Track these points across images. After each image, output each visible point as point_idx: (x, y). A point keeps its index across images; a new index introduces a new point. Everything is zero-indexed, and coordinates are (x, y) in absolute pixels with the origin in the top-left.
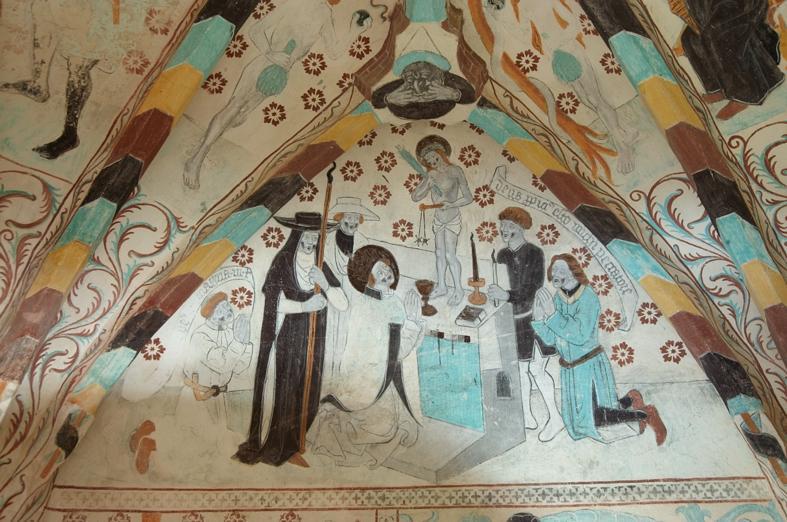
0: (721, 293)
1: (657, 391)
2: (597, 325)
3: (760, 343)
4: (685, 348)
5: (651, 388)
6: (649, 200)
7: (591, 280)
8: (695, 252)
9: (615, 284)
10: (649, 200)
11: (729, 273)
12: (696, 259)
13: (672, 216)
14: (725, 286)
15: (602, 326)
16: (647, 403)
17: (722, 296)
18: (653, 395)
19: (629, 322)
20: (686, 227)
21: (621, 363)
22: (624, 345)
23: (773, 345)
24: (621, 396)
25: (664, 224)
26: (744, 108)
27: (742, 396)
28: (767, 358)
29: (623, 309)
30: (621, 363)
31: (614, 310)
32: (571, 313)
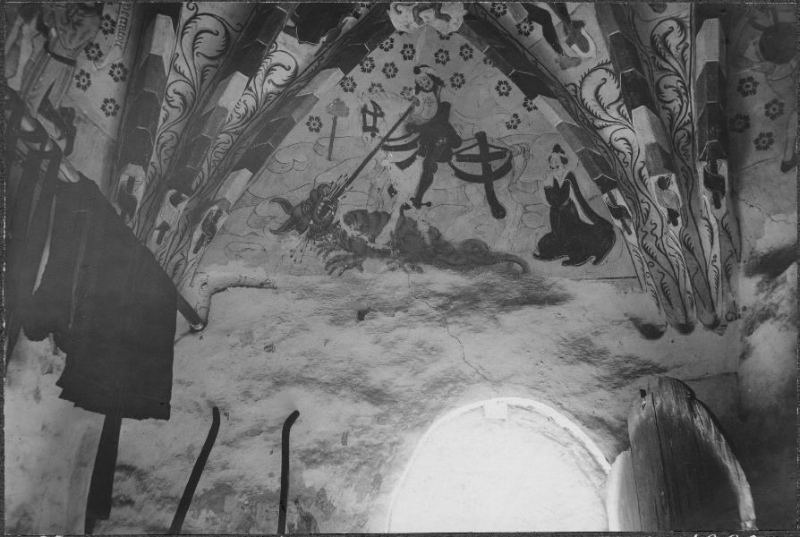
0: (172, 103)
1: (85, 122)
2: (84, 46)
3: (163, 146)
4: (119, 112)
5: (82, 117)
6: (195, 16)
7: (104, 13)
8: (184, 68)
9: (116, 34)
10: (195, 16)
11: (187, 98)
12: (180, 73)
13: (196, 39)
14: (177, 101)
15: (87, 50)
16: (75, 125)
17: (170, 105)
18: (81, 123)
19: (103, 65)
20: (195, 52)
21: (78, 85)
22: (88, 76)
23: (170, 153)
24: (64, 105)
25: (186, 36)
26: (294, 36)
27: (141, 168)
28: (159, 156)
29: (107, 54)
30: (78, 85)
31: (102, 48)
32: (76, 18)
